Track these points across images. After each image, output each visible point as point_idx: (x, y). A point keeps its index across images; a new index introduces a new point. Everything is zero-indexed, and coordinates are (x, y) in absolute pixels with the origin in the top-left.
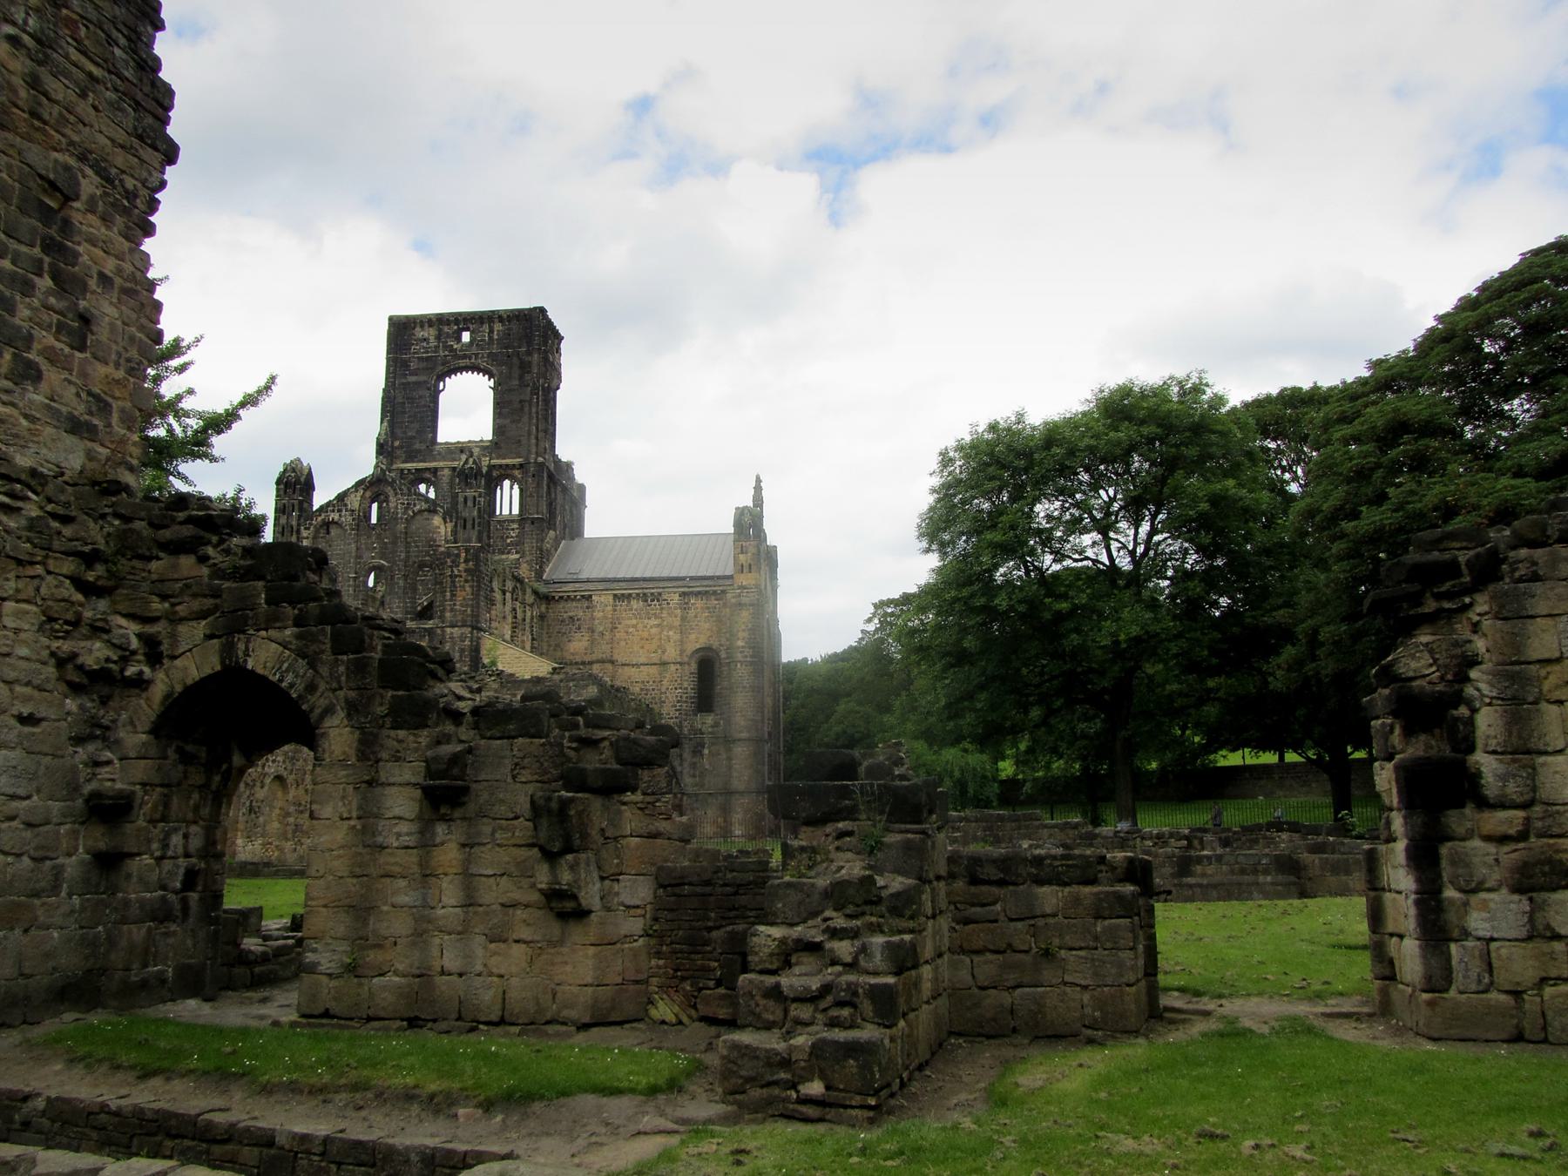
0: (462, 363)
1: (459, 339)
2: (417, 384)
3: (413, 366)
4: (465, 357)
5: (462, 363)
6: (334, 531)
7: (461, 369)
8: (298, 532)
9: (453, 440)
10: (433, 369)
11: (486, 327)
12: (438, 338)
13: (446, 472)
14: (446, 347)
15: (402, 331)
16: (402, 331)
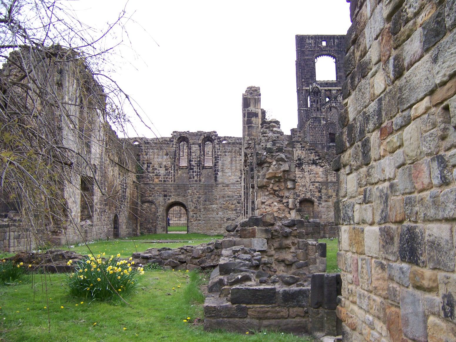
0: (325, 53)
1: (322, 44)
2: (308, 59)
3: (307, 53)
4: (325, 51)
5: (325, 53)
6: (334, 110)
7: (323, 55)
8: (321, 110)
9: (322, 80)
10: (314, 54)
11: (332, 40)
12: (315, 43)
13: (323, 91)
14: (318, 47)
15: (301, 40)
16: (301, 40)
